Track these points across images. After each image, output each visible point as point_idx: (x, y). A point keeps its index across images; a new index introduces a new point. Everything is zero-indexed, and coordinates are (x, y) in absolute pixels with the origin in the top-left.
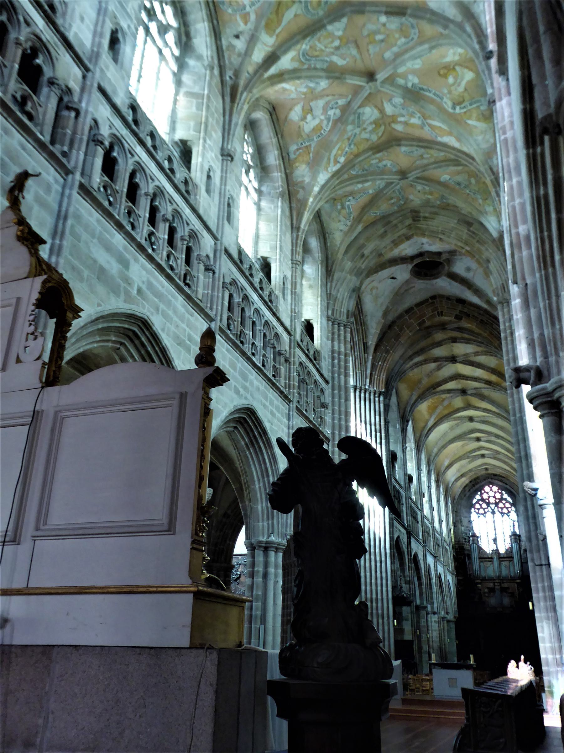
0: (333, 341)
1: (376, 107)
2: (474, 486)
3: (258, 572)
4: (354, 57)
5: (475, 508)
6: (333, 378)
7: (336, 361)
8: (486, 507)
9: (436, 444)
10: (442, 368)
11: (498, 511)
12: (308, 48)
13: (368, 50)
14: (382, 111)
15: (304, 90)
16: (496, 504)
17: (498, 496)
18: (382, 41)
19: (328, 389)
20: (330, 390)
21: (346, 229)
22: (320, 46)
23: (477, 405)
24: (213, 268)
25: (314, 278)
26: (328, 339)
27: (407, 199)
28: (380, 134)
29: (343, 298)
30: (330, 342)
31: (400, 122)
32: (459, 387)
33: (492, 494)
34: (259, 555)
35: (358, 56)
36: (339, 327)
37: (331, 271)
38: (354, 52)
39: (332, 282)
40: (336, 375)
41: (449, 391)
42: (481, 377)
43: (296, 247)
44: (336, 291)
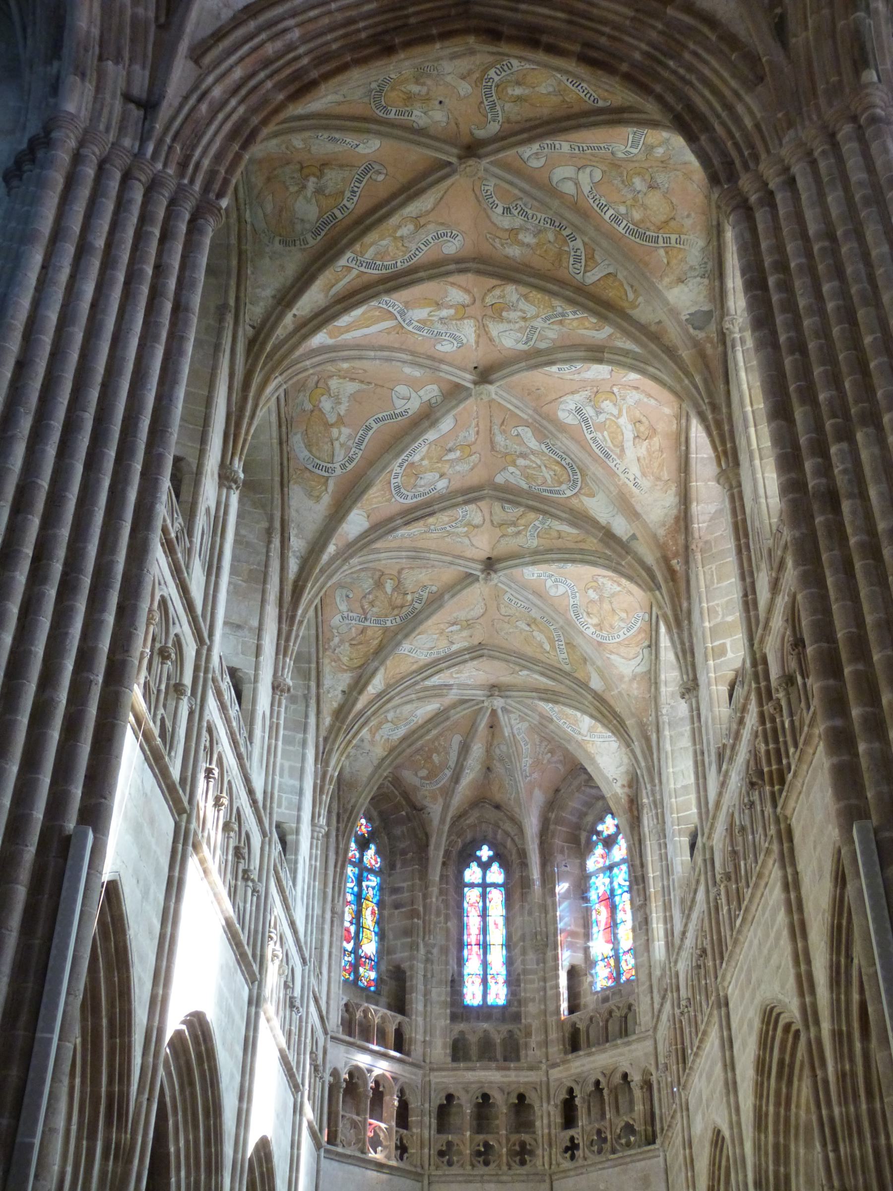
1: (491, 340)
4: (503, 432)
12: (564, 487)
13: (478, 433)
14: (482, 331)
15: (607, 405)
18: (450, 450)
22: (547, 474)
27: (477, 83)
28: (497, 292)
31: (451, 307)
35: (496, 429)
38: (499, 439)
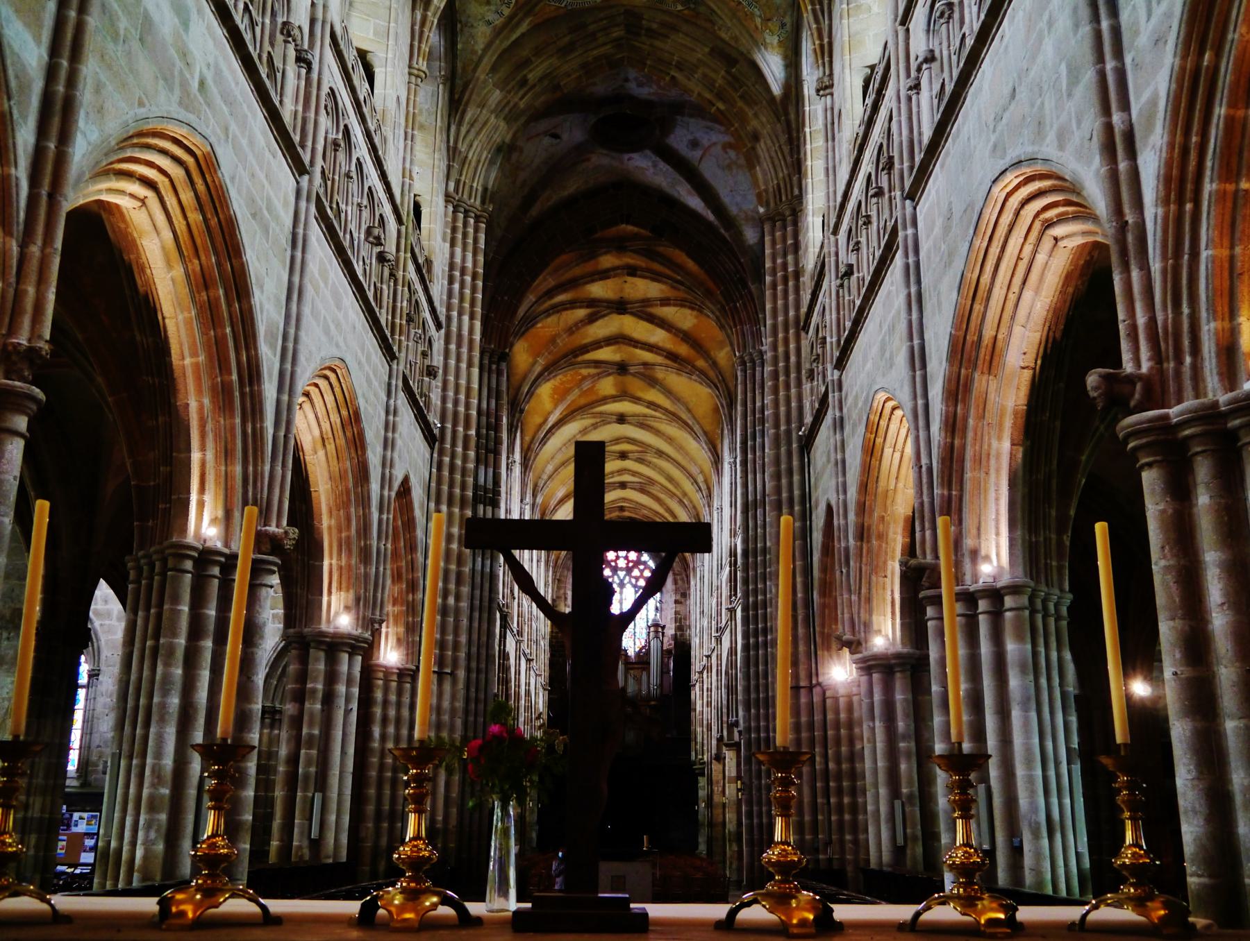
0: (453, 244)
3: (314, 691)
6: (449, 318)
7: (456, 286)
8: (610, 574)
9: (552, 458)
10: (596, 320)
11: (630, 582)
16: (629, 570)
19: (438, 337)
20: (442, 342)
21: (499, 21)
23: (640, 394)
24: (310, 57)
25: (427, 110)
26: (444, 240)
29: (479, 161)
30: (448, 245)
32: (617, 357)
34: (317, 660)
36: (465, 217)
37: (459, 101)
39: (460, 124)
40: (455, 314)
41: (597, 363)
42: (661, 344)
43: (420, 42)
44: (465, 146)
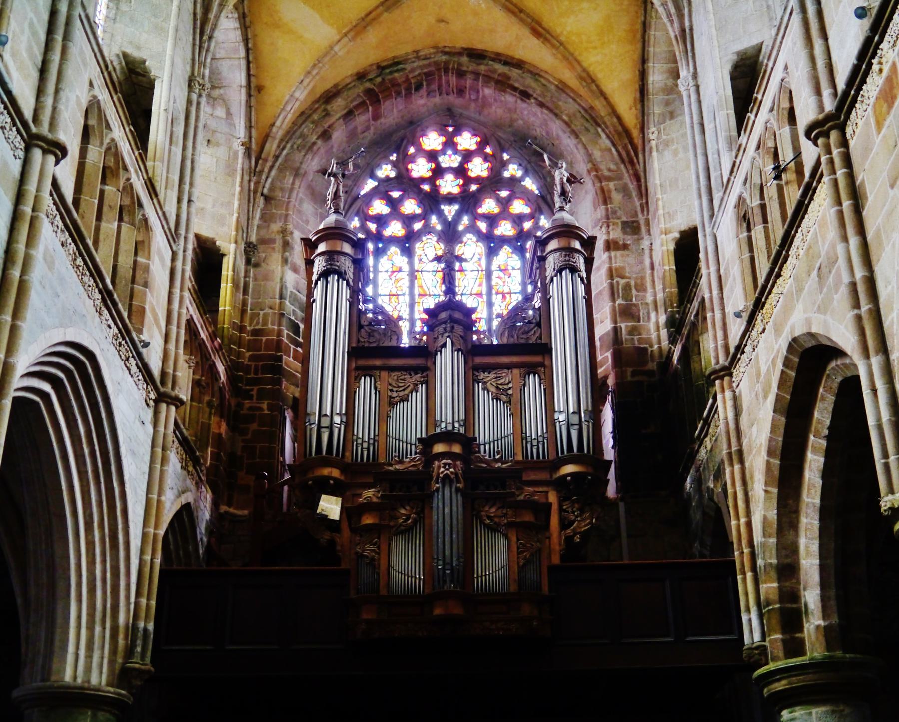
2: (373, 98)
5: (365, 218)
17: (478, 168)
33: (450, 160)
